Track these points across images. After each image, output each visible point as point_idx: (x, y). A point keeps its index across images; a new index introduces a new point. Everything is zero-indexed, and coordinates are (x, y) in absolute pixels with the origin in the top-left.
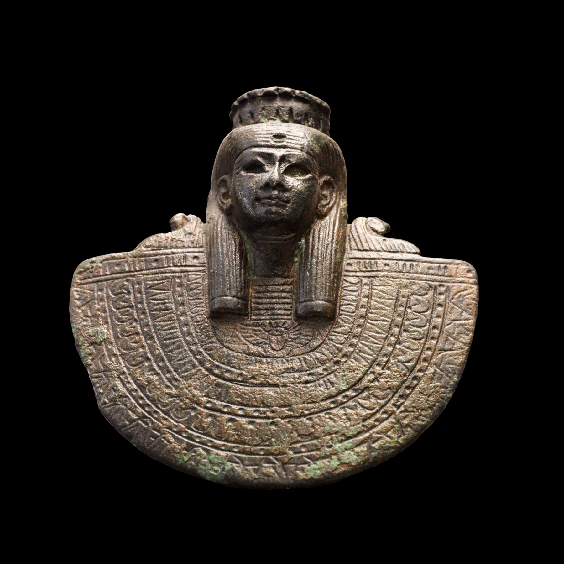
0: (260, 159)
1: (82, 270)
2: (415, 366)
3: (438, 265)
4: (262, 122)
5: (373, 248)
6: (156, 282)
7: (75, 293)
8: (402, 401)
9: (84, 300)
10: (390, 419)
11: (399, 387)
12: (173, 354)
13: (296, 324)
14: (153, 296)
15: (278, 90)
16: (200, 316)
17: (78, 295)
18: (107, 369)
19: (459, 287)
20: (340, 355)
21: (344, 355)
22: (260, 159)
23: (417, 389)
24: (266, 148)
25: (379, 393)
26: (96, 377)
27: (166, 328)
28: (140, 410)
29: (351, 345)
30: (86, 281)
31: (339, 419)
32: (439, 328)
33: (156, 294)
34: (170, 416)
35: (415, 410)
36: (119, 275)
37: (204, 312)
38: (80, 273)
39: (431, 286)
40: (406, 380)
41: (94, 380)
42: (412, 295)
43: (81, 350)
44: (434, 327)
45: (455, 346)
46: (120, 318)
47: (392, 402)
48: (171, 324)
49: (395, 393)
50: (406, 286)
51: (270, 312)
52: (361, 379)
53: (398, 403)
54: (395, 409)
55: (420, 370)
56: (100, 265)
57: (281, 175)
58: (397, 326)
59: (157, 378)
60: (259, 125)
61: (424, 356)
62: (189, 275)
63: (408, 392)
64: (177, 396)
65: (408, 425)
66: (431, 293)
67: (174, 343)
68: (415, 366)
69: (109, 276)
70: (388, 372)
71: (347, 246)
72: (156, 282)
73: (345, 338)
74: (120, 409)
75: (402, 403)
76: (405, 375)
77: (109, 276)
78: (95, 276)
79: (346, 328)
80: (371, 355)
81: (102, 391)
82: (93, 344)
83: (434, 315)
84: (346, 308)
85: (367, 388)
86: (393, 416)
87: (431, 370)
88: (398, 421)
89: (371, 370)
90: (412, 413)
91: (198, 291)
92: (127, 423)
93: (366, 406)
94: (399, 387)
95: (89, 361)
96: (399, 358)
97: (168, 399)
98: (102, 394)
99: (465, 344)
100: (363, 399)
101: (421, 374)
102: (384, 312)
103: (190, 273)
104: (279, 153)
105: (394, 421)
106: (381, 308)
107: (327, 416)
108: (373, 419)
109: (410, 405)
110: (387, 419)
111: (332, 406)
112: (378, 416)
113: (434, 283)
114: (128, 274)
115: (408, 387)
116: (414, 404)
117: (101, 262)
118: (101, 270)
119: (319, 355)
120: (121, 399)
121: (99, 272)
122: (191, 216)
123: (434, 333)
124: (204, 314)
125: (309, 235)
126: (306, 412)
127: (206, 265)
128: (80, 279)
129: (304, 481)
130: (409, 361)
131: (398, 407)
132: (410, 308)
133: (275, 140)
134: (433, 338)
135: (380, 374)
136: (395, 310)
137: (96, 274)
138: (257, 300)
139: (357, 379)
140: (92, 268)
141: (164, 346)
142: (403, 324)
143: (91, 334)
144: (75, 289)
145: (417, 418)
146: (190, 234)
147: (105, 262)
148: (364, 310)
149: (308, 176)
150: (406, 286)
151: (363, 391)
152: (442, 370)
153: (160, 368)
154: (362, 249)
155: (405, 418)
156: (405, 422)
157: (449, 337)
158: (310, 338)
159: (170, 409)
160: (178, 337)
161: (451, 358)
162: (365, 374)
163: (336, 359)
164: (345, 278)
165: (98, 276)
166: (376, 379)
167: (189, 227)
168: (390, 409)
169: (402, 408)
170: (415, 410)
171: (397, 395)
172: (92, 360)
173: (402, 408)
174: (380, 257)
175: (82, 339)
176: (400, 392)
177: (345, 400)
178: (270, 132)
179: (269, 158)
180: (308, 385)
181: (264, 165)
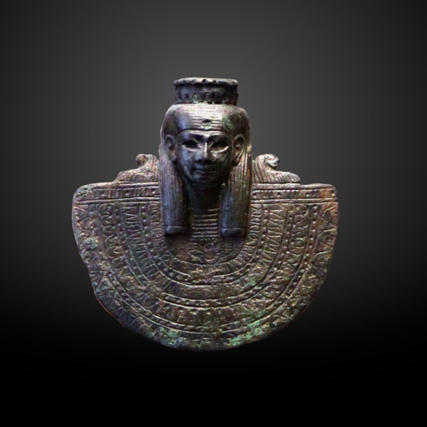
0: (195, 140)
1: (79, 194)
2: (298, 266)
3: (312, 190)
4: (195, 103)
5: (269, 181)
6: (128, 208)
7: (75, 211)
8: (291, 291)
9: (82, 216)
10: (284, 304)
11: (289, 281)
12: (142, 261)
13: (221, 240)
14: (127, 218)
15: (204, 81)
16: (159, 234)
17: (78, 212)
18: (99, 268)
19: (326, 205)
20: (250, 261)
21: (253, 261)
22: (195, 140)
23: (301, 282)
24: (199, 131)
25: (276, 287)
26: (93, 274)
27: (137, 242)
28: (121, 300)
29: (258, 253)
30: (82, 202)
31: (250, 306)
32: (314, 236)
33: (130, 217)
34: (141, 305)
35: (299, 296)
36: (103, 201)
37: (161, 231)
38: (78, 196)
39: (308, 206)
40: (293, 276)
41: (91, 275)
42: (296, 214)
43: (82, 254)
44: (311, 236)
45: (324, 248)
46: (106, 233)
47: (285, 292)
48: (140, 239)
49: (286, 286)
50: (292, 208)
51: (204, 232)
52: (264, 278)
53: (289, 293)
54: (287, 297)
55: (302, 268)
56: (91, 192)
57: (209, 151)
58: (287, 238)
59: (132, 278)
60: (192, 104)
61: (305, 257)
62: (150, 204)
63: (295, 284)
64: (145, 291)
65: (295, 307)
66: (307, 212)
67: (142, 254)
68: (298, 266)
69: (97, 201)
70: (282, 271)
71: (253, 180)
72: (128, 208)
73: (253, 249)
74: (109, 298)
75: (292, 292)
76: (293, 273)
77: (97, 201)
78: (88, 200)
79: (254, 242)
80: (270, 260)
81: (96, 284)
82: (89, 249)
83: (311, 228)
84: (255, 223)
85: (268, 284)
86: (286, 302)
87: (310, 266)
88: (289, 304)
89: (271, 270)
90: (298, 299)
91: (156, 216)
92: (114, 308)
93: (268, 296)
94: (289, 281)
95: (87, 262)
96: (289, 260)
97: (140, 293)
98: (97, 286)
99: (331, 246)
100: (266, 291)
101: (303, 271)
102: (278, 228)
103: (150, 202)
104: (207, 135)
105: (286, 305)
106: (276, 226)
107: (243, 305)
108: (273, 305)
109: (296, 293)
110: (281, 304)
111: (246, 297)
112: (276, 302)
113: (310, 204)
114: (110, 200)
115: (295, 281)
116: (299, 293)
117: (91, 190)
118: (92, 196)
119: (237, 262)
120: (109, 291)
121: (91, 197)
122: (148, 156)
123: (311, 240)
124: (160, 233)
125: (228, 179)
126: (230, 303)
127: (161, 195)
128: (78, 201)
129: (230, 175)
130: (295, 263)
131: (289, 295)
132: (295, 224)
133: (204, 124)
134: (310, 244)
135: (276, 273)
136: (285, 227)
137: (89, 198)
138: (196, 225)
139: (262, 278)
140: (86, 193)
141: (136, 256)
142: (290, 236)
143: (88, 243)
144: (76, 207)
145: (301, 302)
146: (149, 171)
147: (94, 190)
148: (265, 228)
149: (226, 148)
150: (292, 208)
151: (265, 286)
152: (316, 266)
153: (134, 271)
154: (262, 182)
155: (294, 302)
156: (294, 305)
157: (321, 243)
158: (230, 250)
159: (142, 300)
160: (144, 249)
161: (322, 257)
162: (267, 273)
163: (248, 264)
164: (252, 205)
165: (90, 200)
166: (273, 277)
167: (148, 165)
168: (284, 297)
169: (291, 296)
170: (299, 296)
171: (288, 287)
172: (89, 261)
173: (291, 296)
174: (275, 188)
175: (81, 246)
176: (290, 284)
177: (254, 293)
178: (200, 118)
179: (200, 138)
180: (231, 283)
181: (197, 144)
